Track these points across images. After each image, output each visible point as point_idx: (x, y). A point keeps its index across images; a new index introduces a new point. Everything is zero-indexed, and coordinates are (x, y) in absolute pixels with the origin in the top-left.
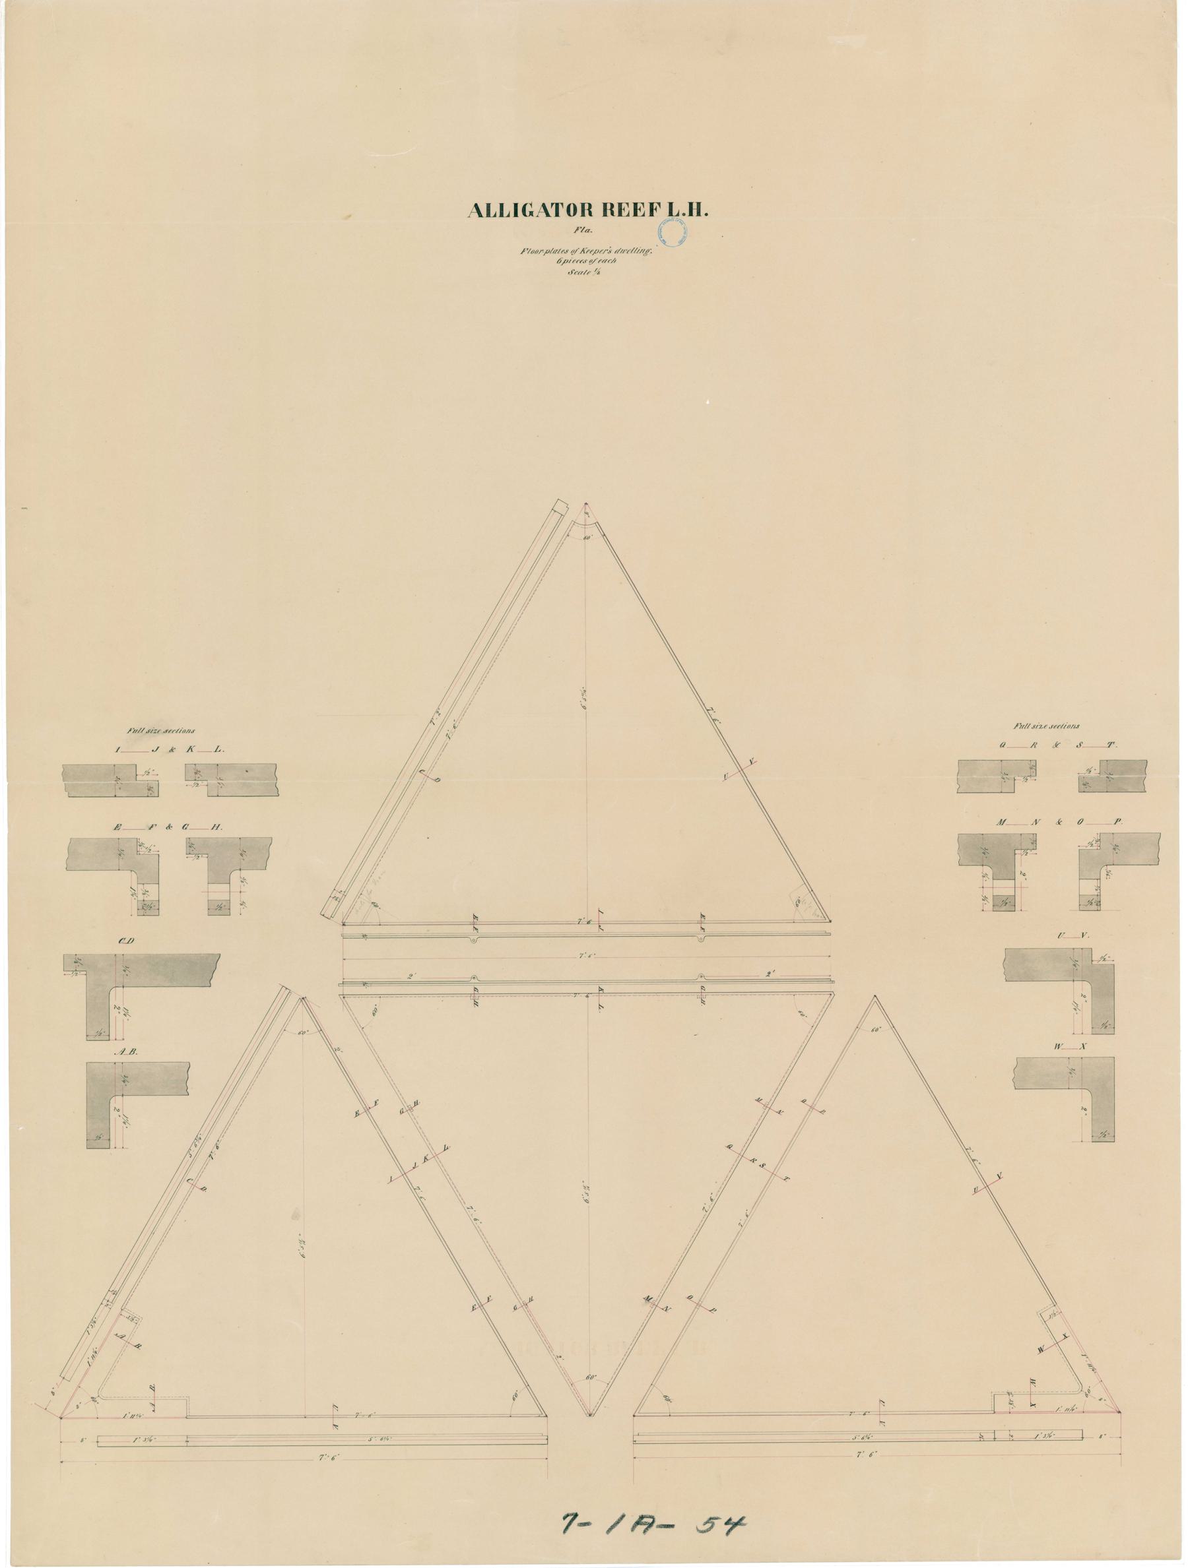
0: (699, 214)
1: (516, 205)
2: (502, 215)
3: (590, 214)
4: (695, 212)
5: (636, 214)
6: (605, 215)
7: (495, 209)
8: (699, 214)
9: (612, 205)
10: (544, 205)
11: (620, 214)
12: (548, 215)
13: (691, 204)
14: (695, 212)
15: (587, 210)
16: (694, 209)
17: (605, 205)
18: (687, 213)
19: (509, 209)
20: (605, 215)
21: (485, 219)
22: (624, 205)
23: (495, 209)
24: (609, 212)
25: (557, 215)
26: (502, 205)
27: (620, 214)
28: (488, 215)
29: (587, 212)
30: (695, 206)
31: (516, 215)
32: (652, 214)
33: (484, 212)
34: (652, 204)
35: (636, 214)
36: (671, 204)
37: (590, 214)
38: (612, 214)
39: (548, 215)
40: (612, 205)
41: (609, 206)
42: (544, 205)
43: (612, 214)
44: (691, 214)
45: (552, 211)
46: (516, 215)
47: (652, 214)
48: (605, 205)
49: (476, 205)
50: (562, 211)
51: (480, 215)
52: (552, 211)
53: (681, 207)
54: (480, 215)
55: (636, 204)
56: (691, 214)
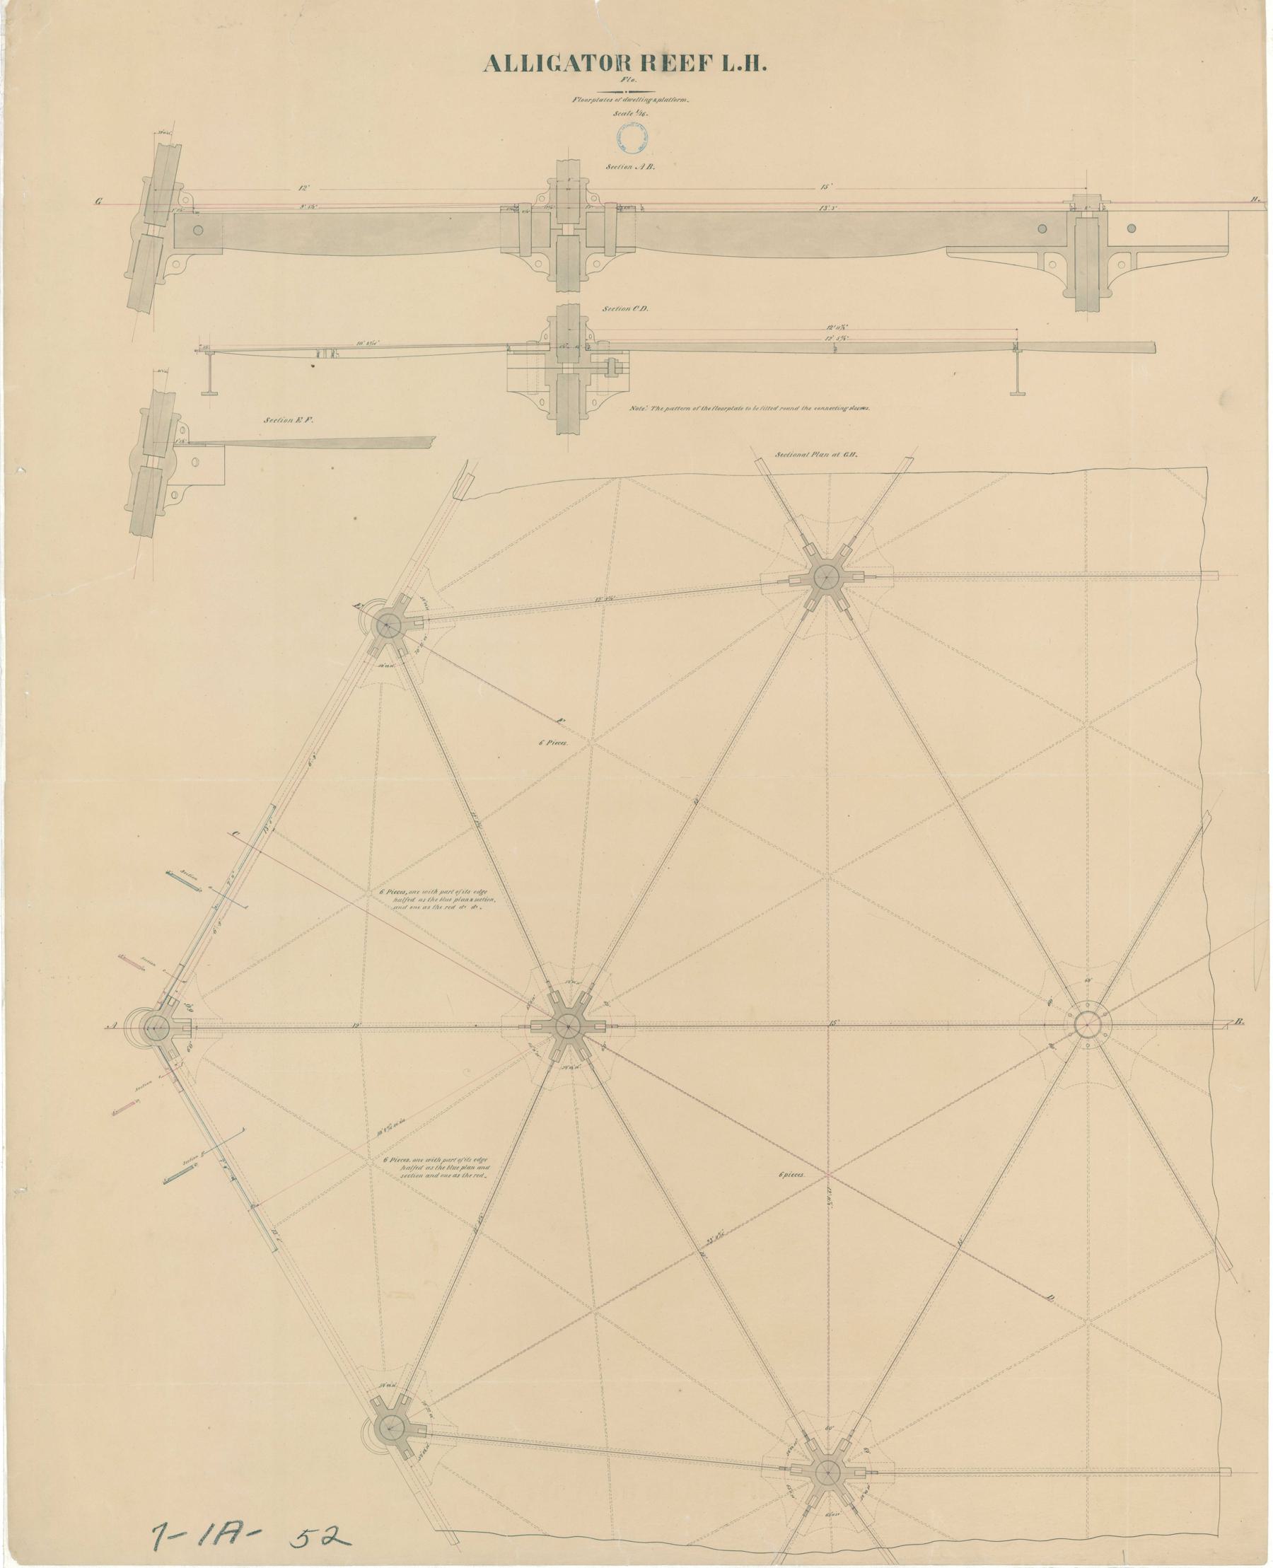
0: (756, 69)
1: (540, 57)
2: (525, 69)
3: (628, 68)
4: (752, 66)
5: (683, 69)
6: (644, 69)
7: (516, 62)
8: (756, 69)
9: (653, 58)
10: (572, 58)
11: (665, 69)
12: (577, 69)
13: (748, 57)
14: (752, 66)
15: (623, 62)
16: (752, 63)
17: (644, 57)
18: (744, 68)
19: (533, 62)
20: (644, 69)
21: (503, 73)
22: (670, 58)
23: (516, 62)
24: (648, 66)
25: (589, 69)
26: (525, 57)
27: (665, 69)
28: (508, 69)
29: (624, 65)
30: (752, 59)
31: (540, 69)
32: (702, 69)
33: (502, 65)
34: (702, 57)
35: (683, 69)
36: (726, 57)
37: (628, 68)
38: (653, 68)
39: (577, 69)
40: (653, 58)
41: (648, 59)
42: (572, 58)
43: (653, 68)
44: (748, 69)
45: (582, 64)
46: (540, 69)
47: (702, 69)
48: (644, 57)
49: (493, 58)
50: (595, 64)
51: (497, 69)
52: (582, 64)
53: (737, 60)
54: (497, 69)
55: (683, 57)
56: (748, 69)
